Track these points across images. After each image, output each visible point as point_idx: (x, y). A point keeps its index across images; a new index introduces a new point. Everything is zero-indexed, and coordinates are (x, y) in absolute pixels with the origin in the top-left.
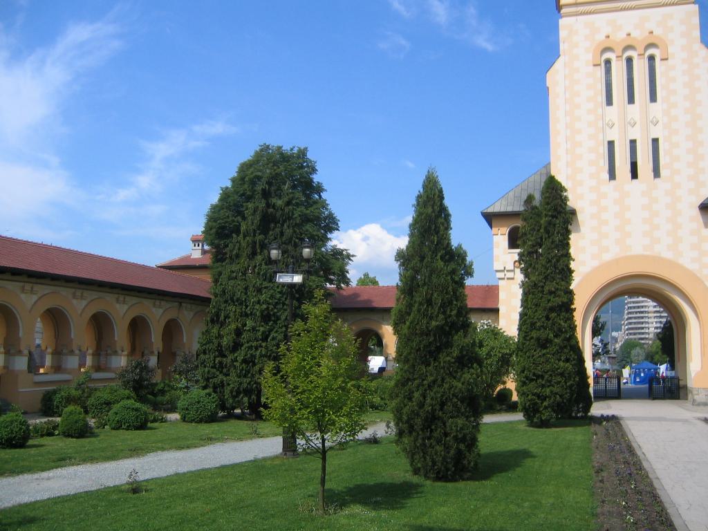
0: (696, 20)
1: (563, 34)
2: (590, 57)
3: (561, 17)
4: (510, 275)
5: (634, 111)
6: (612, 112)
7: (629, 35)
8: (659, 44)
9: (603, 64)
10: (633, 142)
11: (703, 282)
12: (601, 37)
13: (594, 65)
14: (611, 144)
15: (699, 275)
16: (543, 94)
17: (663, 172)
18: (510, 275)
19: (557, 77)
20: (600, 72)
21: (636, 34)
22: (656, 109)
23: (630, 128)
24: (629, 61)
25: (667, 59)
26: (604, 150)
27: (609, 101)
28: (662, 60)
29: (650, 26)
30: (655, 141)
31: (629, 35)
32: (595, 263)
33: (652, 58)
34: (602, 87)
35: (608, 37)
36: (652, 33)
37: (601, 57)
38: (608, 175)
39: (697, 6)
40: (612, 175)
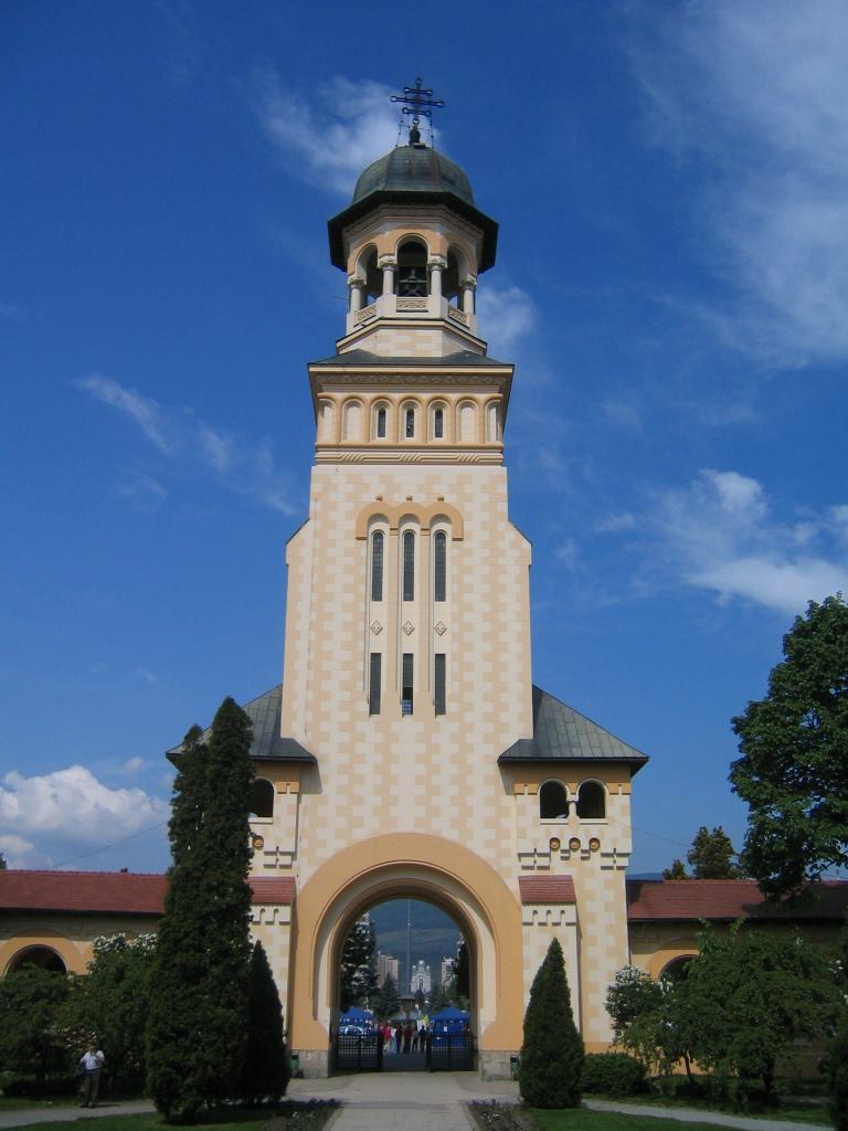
0: (503, 489)
1: (315, 487)
2: (352, 525)
5: (412, 611)
6: (380, 611)
7: (410, 499)
8: (452, 518)
9: (371, 539)
10: (408, 658)
11: (500, 879)
13: (358, 539)
14: (376, 657)
15: (495, 868)
16: (281, 571)
17: (450, 706)
19: (302, 552)
21: (419, 499)
22: (443, 611)
23: (372, 635)
24: (409, 536)
25: (461, 540)
26: (364, 666)
27: (377, 595)
28: (454, 540)
29: (440, 489)
30: (440, 658)
31: (410, 499)
32: (342, 844)
33: (441, 536)
34: (366, 571)
35: (380, 499)
36: (442, 499)
37: (369, 525)
38: (368, 706)
39: (505, 468)
40: (374, 707)
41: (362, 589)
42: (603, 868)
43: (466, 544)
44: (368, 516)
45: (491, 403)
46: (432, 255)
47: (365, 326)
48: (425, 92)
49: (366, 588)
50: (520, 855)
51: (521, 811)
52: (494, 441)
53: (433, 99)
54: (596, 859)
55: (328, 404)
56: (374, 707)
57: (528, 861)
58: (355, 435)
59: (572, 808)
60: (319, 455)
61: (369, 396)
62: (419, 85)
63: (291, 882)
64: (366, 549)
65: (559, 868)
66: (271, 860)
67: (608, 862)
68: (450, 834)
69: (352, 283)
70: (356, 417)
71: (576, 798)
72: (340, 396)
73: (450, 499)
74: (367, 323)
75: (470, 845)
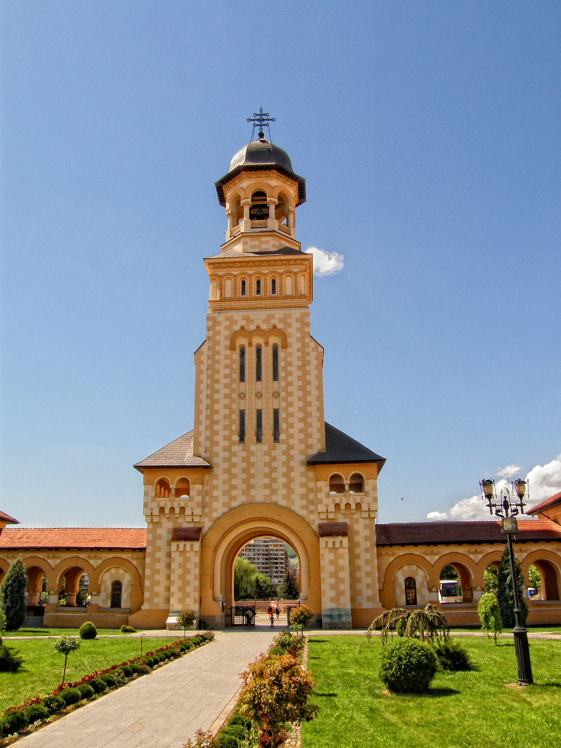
12: (236, 328)
21: (264, 327)
26: (236, 417)
32: (226, 509)
40: (242, 439)
43: (289, 350)
46: (269, 197)
47: (235, 237)
48: (265, 115)
49: (236, 376)
56: (242, 439)
62: (261, 111)
64: (236, 356)
65: (341, 519)
68: (283, 503)
73: (280, 326)
74: (236, 235)
75: (293, 508)
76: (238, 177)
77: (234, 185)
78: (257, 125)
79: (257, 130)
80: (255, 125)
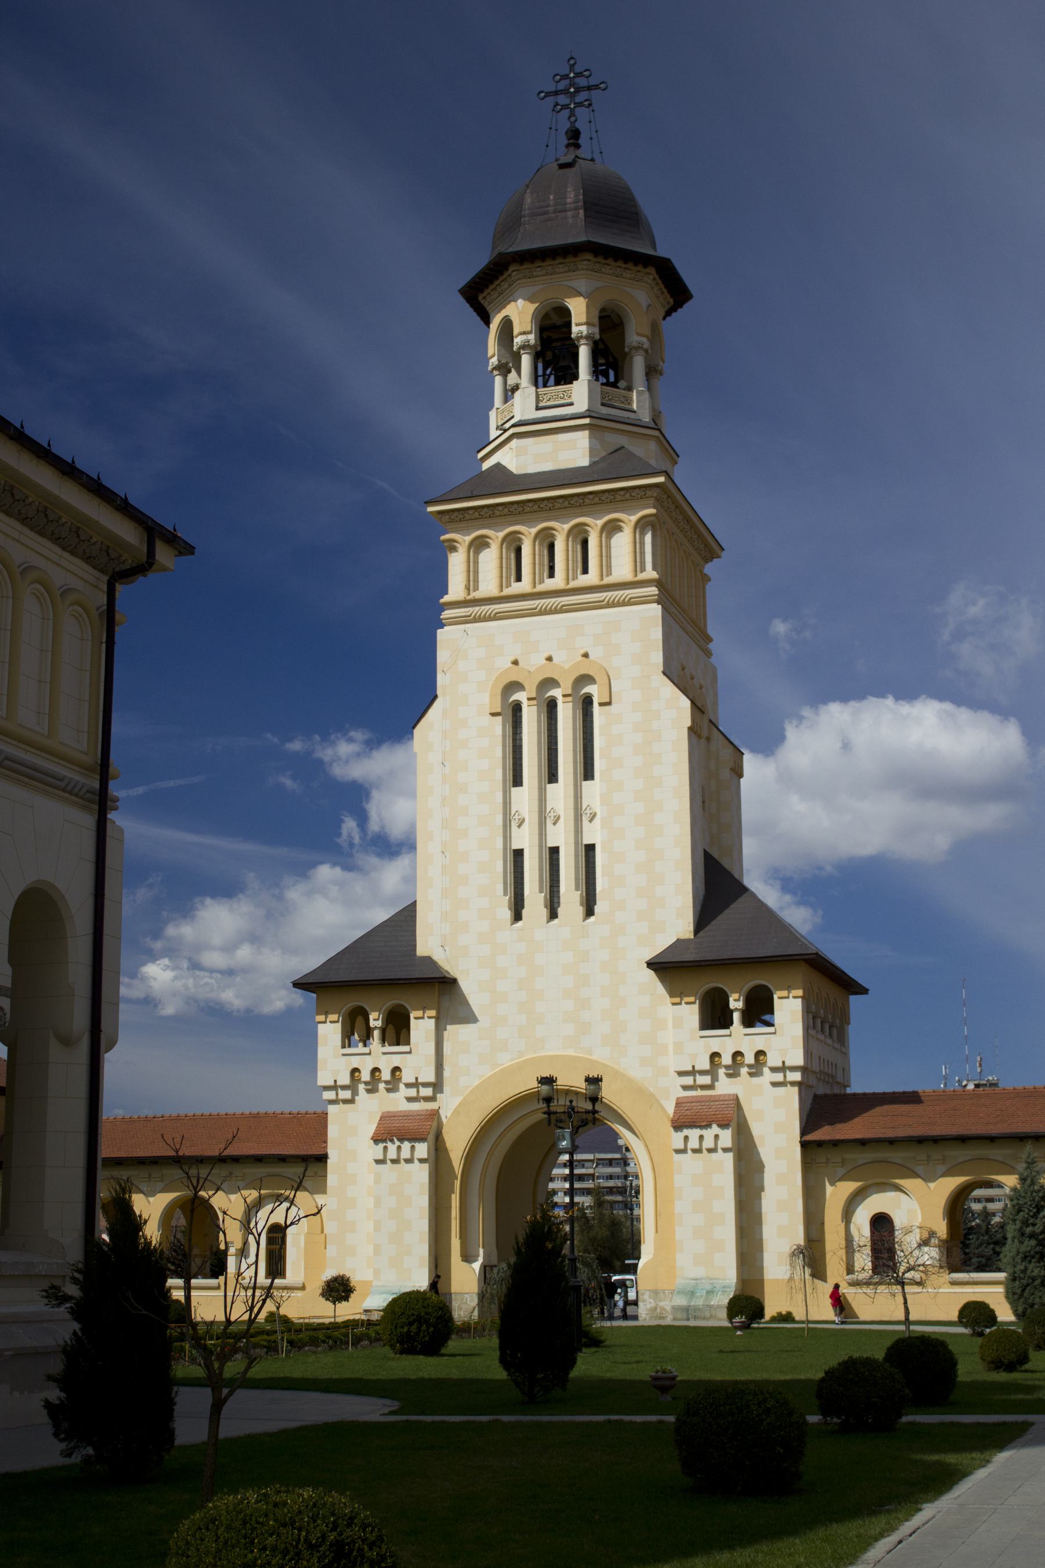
0: (657, 633)
1: (442, 656)
3: (442, 626)
4: (346, 1094)
11: (657, 1101)
13: (493, 714)
18: (346, 1094)
20: (497, 727)
24: (551, 706)
25: (609, 703)
28: (601, 704)
29: (583, 644)
30: (590, 849)
31: (550, 659)
33: (588, 701)
39: (660, 606)
41: (499, 774)
42: (775, 1084)
44: (501, 686)
45: (641, 526)
50: (681, 1074)
51: (678, 1023)
52: (650, 573)
53: (593, 81)
54: (768, 1076)
55: (454, 549)
56: (517, 917)
57: (688, 1080)
58: (489, 585)
59: (736, 1017)
60: (446, 614)
61: (496, 536)
63: (435, 1114)
66: (412, 1092)
67: (779, 1077)
69: (494, 369)
70: (490, 560)
71: (740, 1005)
72: (463, 540)
76: (505, 276)
77: (500, 294)
78: (565, 107)
79: (563, 123)
80: (557, 108)
